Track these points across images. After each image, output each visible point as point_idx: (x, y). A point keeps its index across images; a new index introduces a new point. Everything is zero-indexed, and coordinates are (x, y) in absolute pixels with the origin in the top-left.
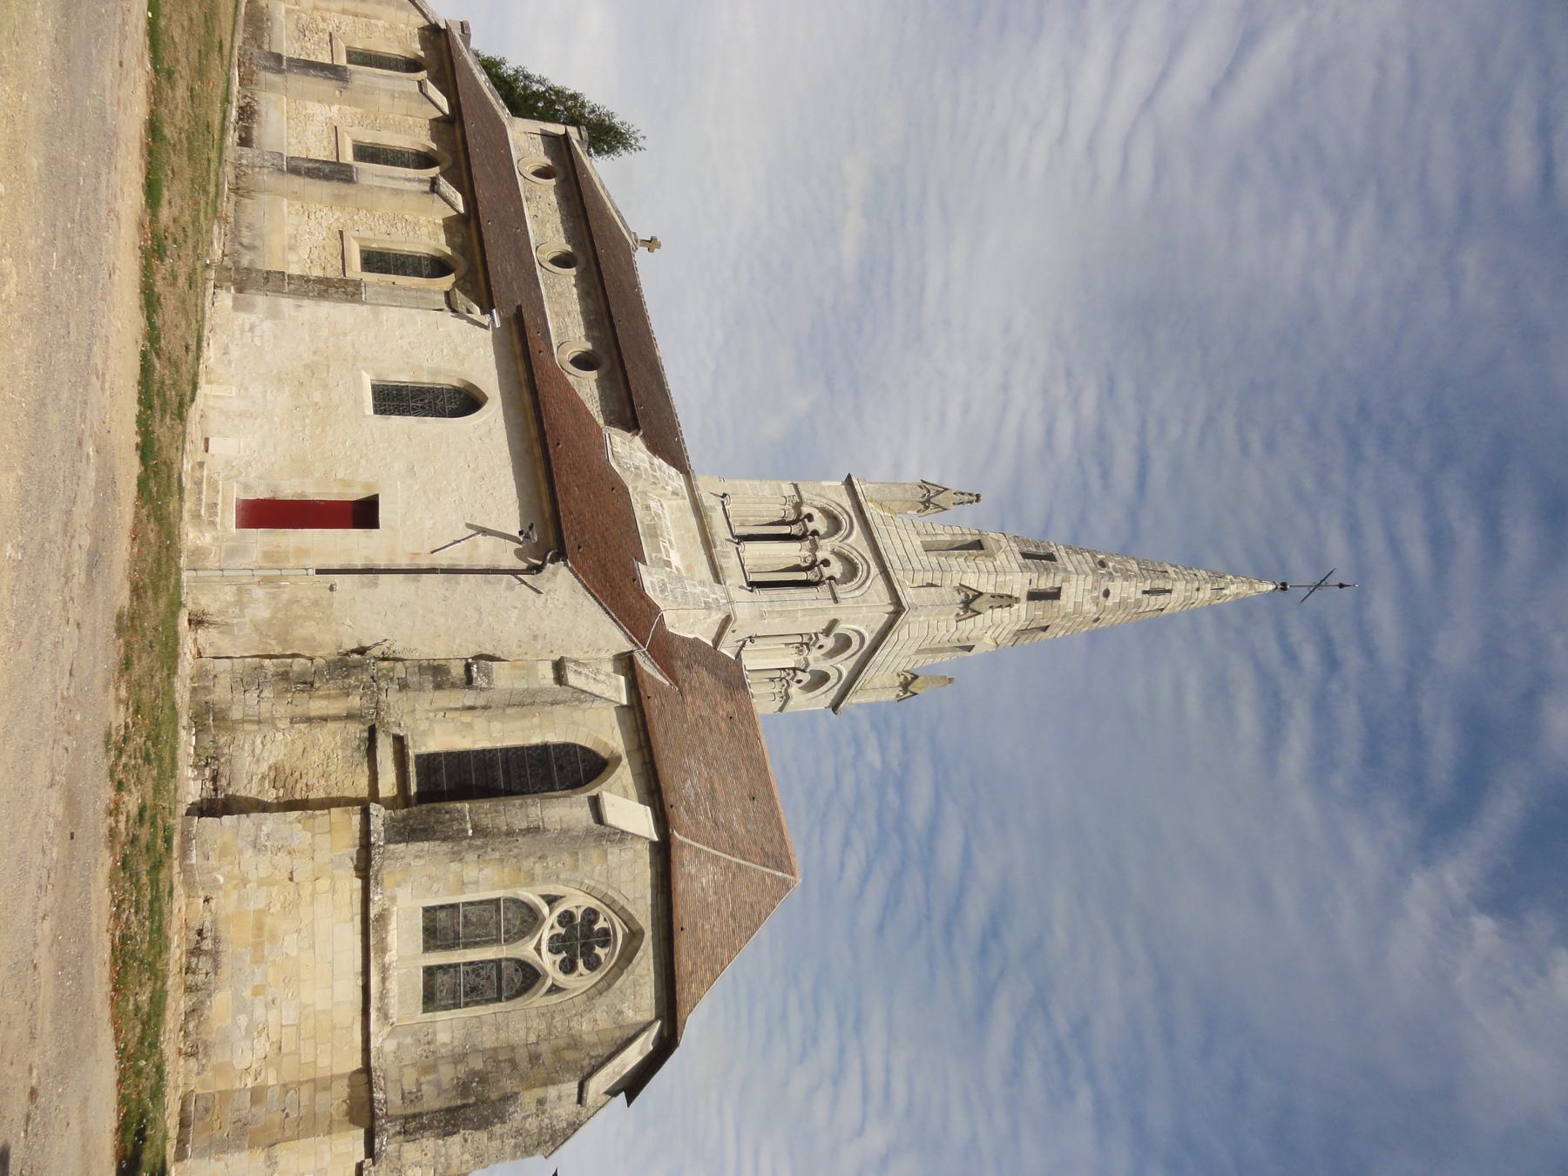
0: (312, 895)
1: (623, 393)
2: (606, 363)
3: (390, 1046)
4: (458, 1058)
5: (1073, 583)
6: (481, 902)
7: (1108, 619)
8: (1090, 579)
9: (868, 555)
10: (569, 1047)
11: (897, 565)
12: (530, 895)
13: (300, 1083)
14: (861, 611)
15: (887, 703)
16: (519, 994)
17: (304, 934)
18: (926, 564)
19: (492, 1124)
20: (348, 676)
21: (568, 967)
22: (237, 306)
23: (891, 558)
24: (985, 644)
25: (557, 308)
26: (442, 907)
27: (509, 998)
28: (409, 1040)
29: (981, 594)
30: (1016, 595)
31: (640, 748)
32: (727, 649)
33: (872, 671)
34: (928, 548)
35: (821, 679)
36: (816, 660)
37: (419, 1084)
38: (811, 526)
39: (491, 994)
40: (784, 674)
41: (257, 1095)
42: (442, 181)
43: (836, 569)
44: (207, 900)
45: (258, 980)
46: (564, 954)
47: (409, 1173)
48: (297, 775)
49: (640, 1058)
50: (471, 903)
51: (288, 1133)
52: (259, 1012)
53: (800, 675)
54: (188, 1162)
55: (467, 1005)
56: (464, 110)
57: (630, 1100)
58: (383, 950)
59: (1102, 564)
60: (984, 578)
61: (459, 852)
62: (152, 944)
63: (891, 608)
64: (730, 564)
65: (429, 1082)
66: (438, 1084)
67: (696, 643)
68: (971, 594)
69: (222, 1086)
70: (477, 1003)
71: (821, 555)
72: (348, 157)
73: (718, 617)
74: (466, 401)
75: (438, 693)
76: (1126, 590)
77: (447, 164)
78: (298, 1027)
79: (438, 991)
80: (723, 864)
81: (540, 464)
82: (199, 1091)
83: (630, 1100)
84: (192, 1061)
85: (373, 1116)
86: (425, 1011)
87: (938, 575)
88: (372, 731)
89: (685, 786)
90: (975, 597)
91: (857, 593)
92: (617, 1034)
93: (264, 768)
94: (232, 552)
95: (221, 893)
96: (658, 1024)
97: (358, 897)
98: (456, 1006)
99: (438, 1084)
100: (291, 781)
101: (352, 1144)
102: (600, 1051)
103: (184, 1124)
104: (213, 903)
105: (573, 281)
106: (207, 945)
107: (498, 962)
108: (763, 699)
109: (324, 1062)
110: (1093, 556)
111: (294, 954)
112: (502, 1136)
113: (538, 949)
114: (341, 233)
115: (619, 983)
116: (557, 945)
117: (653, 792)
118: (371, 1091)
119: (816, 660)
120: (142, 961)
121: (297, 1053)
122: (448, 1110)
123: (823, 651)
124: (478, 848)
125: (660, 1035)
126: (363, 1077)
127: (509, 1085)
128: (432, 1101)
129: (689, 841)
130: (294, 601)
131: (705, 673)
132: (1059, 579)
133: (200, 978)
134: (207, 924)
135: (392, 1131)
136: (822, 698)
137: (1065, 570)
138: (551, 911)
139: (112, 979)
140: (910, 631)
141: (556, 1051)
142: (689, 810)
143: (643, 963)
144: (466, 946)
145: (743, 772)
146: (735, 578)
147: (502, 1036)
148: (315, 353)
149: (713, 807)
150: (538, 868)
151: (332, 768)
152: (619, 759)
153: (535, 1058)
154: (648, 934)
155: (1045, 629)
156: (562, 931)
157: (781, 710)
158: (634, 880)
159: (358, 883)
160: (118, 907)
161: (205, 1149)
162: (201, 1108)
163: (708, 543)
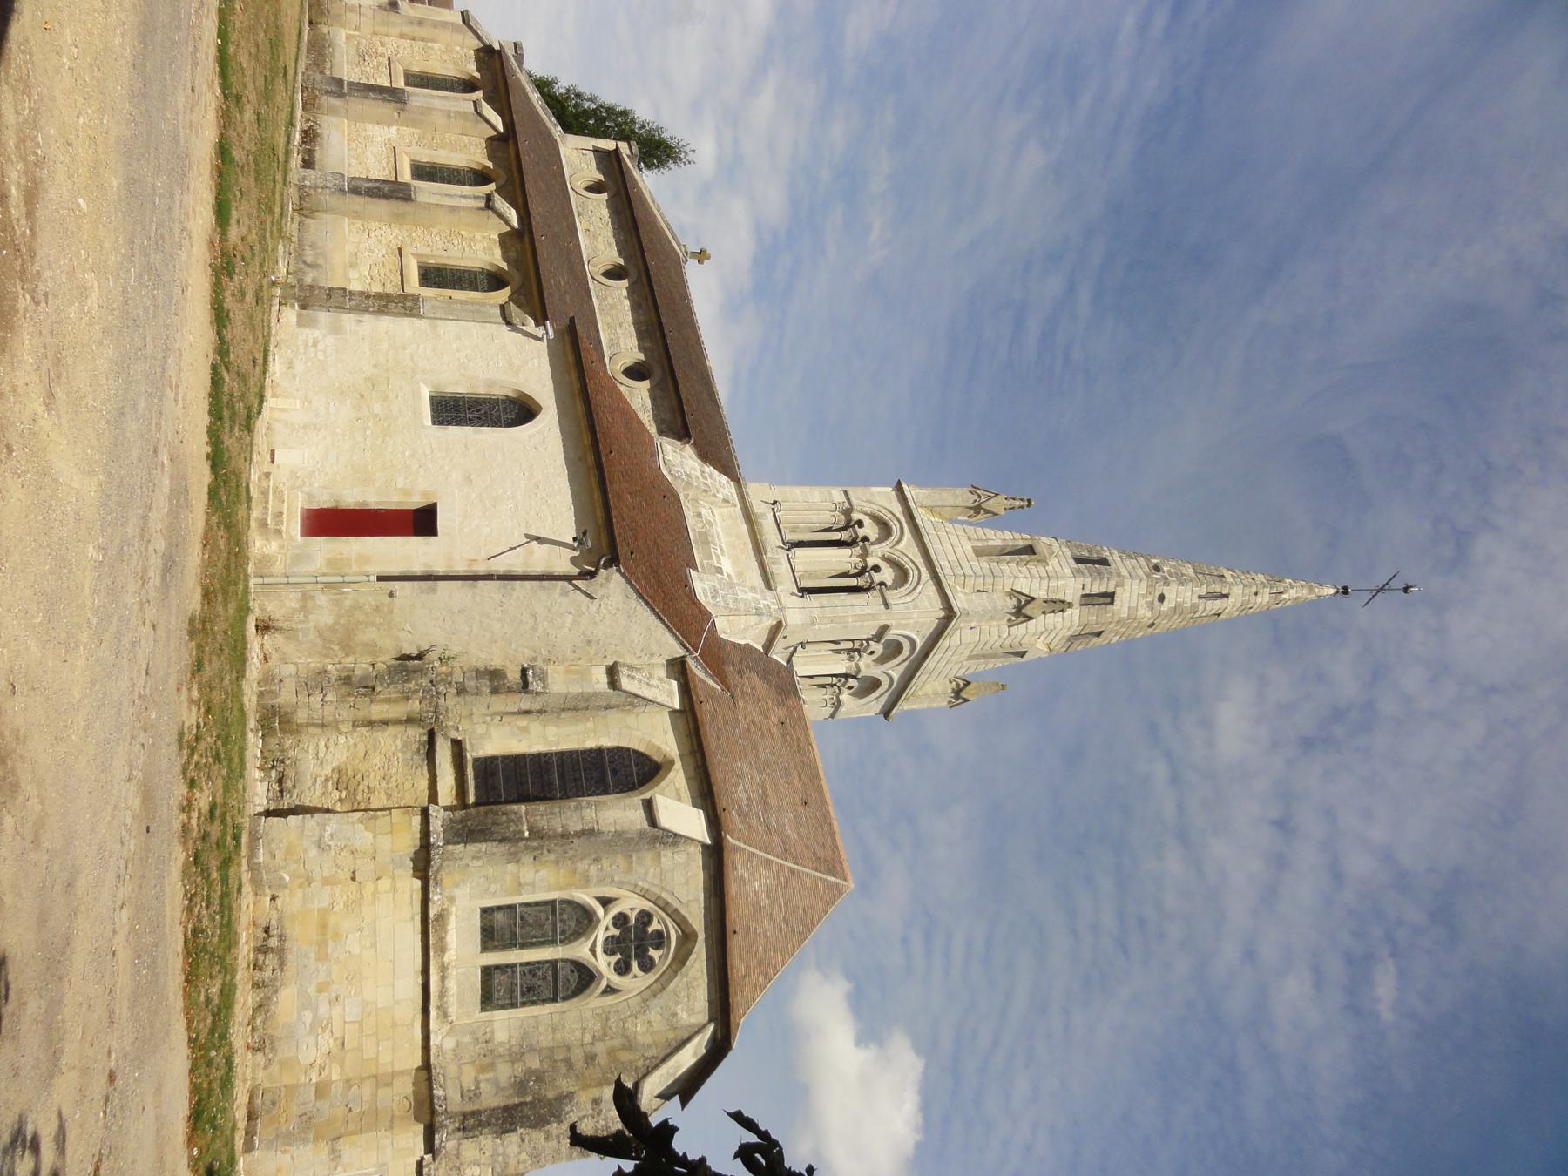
0: (374, 894)
1: (675, 402)
2: (658, 373)
3: (449, 1044)
4: (516, 1056)
5: (1127, 587)
6: (537, 904)
7: (1164, 625)
8: (1144, 584)
9: (919, 561)
10: (624, 1048)
11: (948, 571)
12: (586, 897)
13: (362, 1079)
14: (912, 613)
15: (939, 710)
16: (574, 994)
17: (366, 932)
18: (977, 569)
19: (548, 1123)
20: (408, 681)
21: (623, 969)
22: (300, 324)
23: (942, 563)
24: (1040, 648)
25: (609, 319)
26: (499, 908)
27: (564, 999)
28: (467, 1039)
29: (1033, 599)
30: (1068, 599)
31: (692, 752)
32: (778, 656)
33: (924, 678)
34: (979, 553)
35: (872, 685)
36: (868, 666)
37: (477, 1082)
38: (861, 532)
39: (547, 994)
40: (835, 680)
41: (322, 1090)
42: (497, 197)
43: (887, 574)
44: (273, 898)
45: (322, 977)
46: (619, 956)
47: (468, 1171)
48: (359, 777)
49: (693, 1061)
50: (527, 905)
51: (351, 1127)
52: (323, 1009)
53: (852, 682)
54: (256, 1153)
55: (524, 1004)
56: (518, 128)
57: (684, 1103)
58: (443, 950)
59: (1157, 569)
60: (1036, 583)
61: (516, 854)
62: (222, 938)
63: (942, 614)
64: (781, 570)
65: (487, 1080)
66: (496, 1082)
67: (748, 649)
68: (1023, 599)
69: (288, 1080)
70: (534, 1003)
71: (871, 561)
72: (406, 176)
73: (769, 622)
74: (521, 411)
75: (494, 698)
76: (1181, 595)
77: (502, 182)
78: (361, 1023)
79: (496, 990)
80: (775, 868)
81: (594, 472)
82: (267, 1085)
83: (684, 1103)
84: (259, 1056)
85: (433, 1112)
86: (483, 1010)
87: (989, 580)
88: (431, 735)
89: (737, 791)
90: (1027, 603)
91: (908, 599)
92: (671, 1035)
93: (328, 770)
94: (298, 559)
95: (287, 892)
96: (711, 1027)
97: (417, 896)
98: (513, 1005)
99: (496, 1082)
100: (353, 783)
101: (414, 1139)
102: (653, 1052)
103: (251, 1116)
104: (279, 901)
105: (625, 293)
106: (273, 942)
107: (554, 963)
108: (814, 704)
109: (385, 1058)
110: (1147, 561)
111: (356, 951)
112: (558, 1137)
113: (593, 950)
115: (672, 985)
116: (612, 946)
117: (706, 795)
118: (431, 1089)
119: (867, 666)
120: (212, 954)
121: (360, 1049)
122: (506, 1109)
123: (874, 657)
124: (535, 849)
125: (713, 1039)
126: (424, 1074)
127: (565, 1085)
128: (490, 1099)
129: (742, 845)
130: (356, 607)
131: (756, 679)
132: (1112, 583)
133: (267, 974)
134: (274, 922)
135: (451, 1128)
136: (873, 704)
137: (1119, 575)
138: (606, 913)
139: (184, 970)
140: (959, 637)
141: (611, 1052)
142: (741, 813)
143: (697, 966)
144: (523, 946)
145: (795, 777)
146: (785, 585)
147: (558, 1036)
148: (375, 366)
149: (765, 811)
150: (593, 870)
151: (393, 770)
152: (672, 763)
153: (590, 1058)
154: (701, 936)
155: (1099, 634)
156: (617, 933)
157: (832, 716)
158: (687, 883)
159: (418, 883)
160: (191, 900)
161: (271, 1142)
162: (268, 1103)
163: (759, 550)
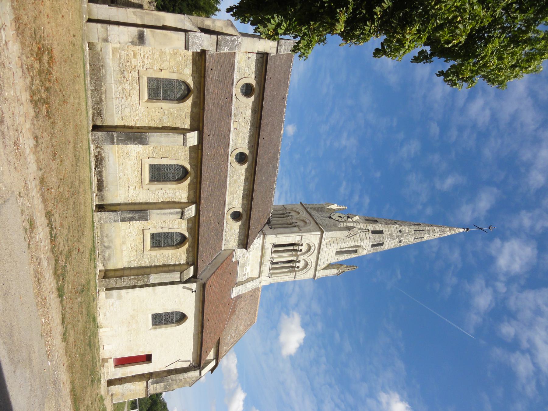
1: (246, 233)
2: (244, 217)
22: (107, 298)
74: (181, 318)
81: (200, 340)
114: (143, 230)
148: (134, 310)
163: (261, 263)
